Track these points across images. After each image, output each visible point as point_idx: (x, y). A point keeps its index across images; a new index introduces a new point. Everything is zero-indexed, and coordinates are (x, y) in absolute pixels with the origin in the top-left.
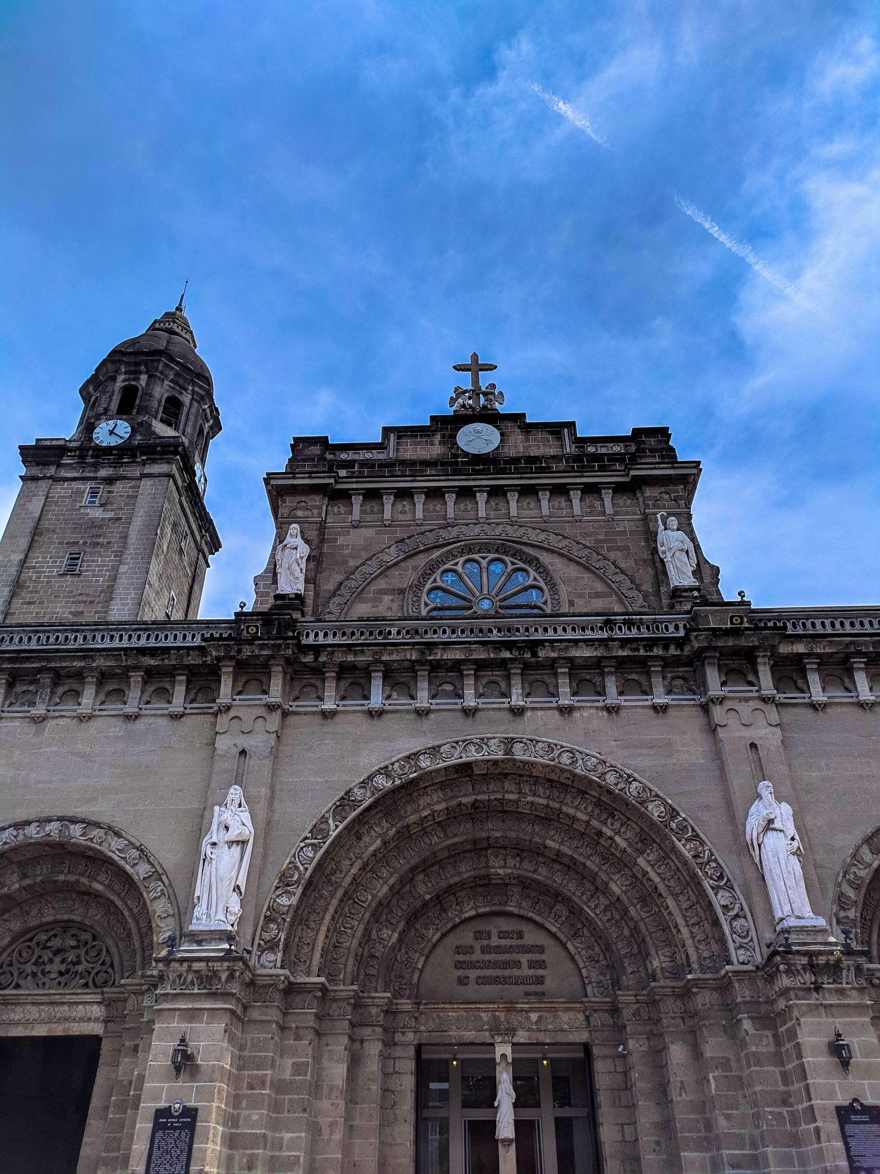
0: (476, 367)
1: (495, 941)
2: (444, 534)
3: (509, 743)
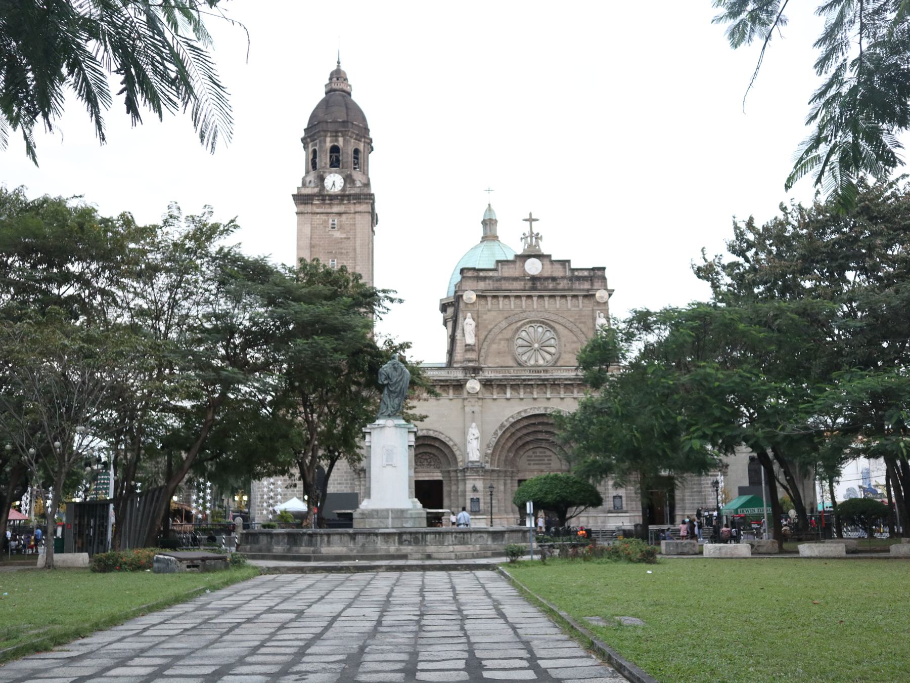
0: (531, 220)
1: (538, 454)
2: (521, 315)
3: (546, 408)
